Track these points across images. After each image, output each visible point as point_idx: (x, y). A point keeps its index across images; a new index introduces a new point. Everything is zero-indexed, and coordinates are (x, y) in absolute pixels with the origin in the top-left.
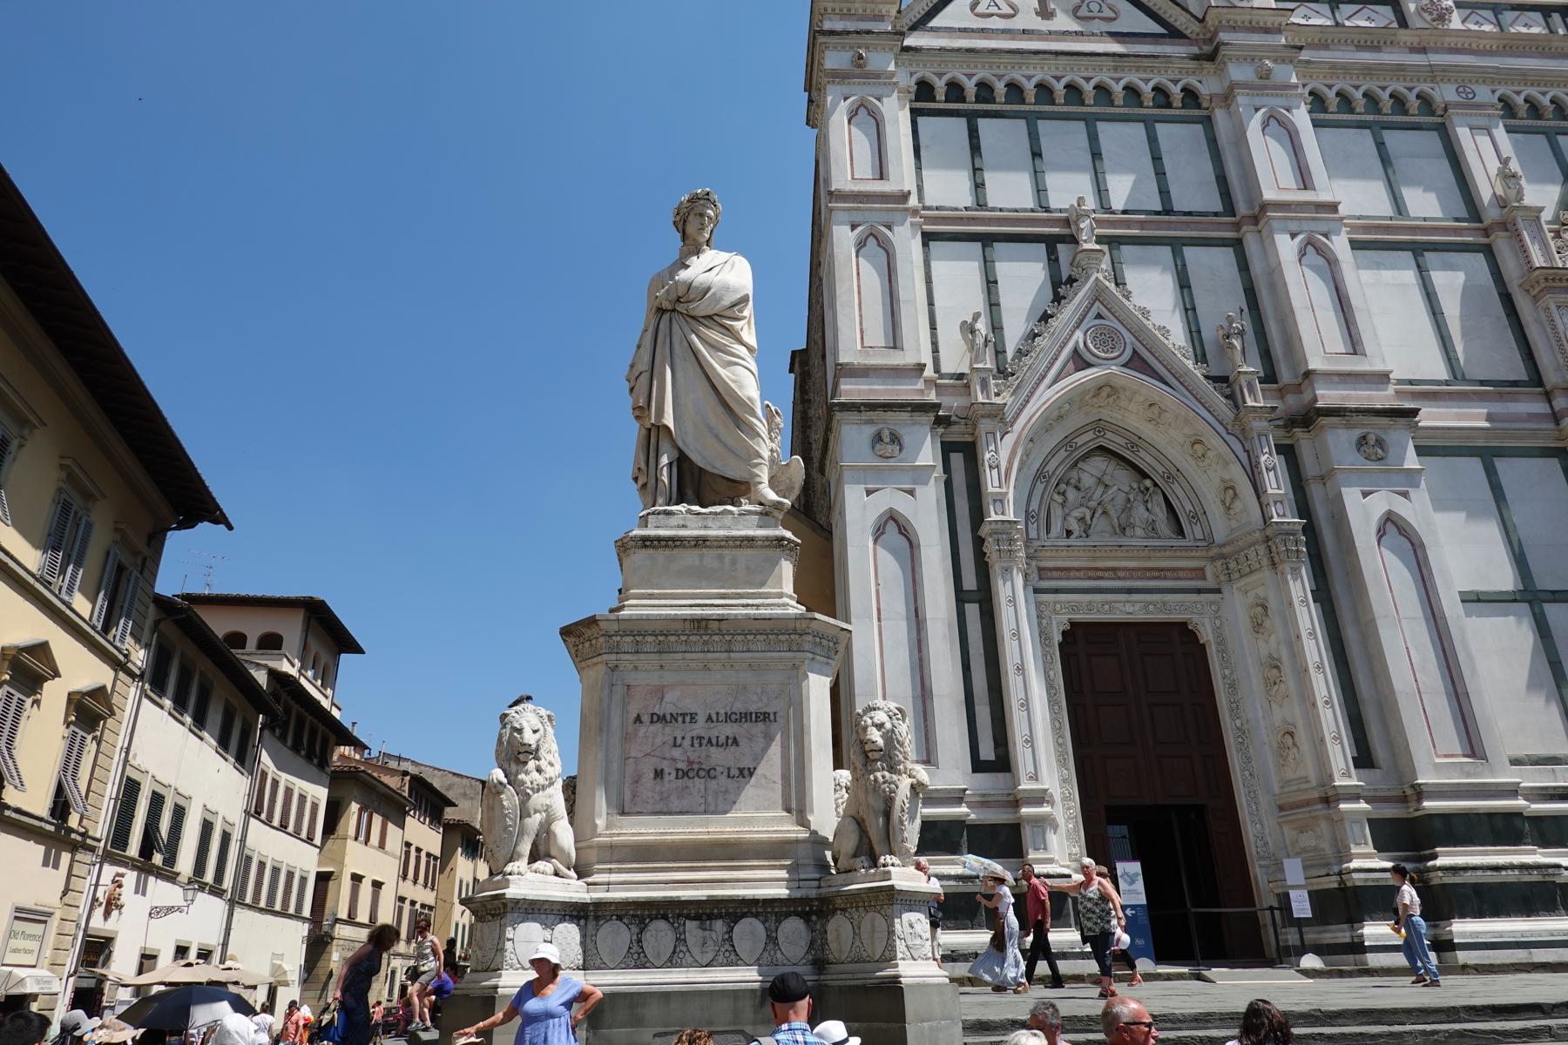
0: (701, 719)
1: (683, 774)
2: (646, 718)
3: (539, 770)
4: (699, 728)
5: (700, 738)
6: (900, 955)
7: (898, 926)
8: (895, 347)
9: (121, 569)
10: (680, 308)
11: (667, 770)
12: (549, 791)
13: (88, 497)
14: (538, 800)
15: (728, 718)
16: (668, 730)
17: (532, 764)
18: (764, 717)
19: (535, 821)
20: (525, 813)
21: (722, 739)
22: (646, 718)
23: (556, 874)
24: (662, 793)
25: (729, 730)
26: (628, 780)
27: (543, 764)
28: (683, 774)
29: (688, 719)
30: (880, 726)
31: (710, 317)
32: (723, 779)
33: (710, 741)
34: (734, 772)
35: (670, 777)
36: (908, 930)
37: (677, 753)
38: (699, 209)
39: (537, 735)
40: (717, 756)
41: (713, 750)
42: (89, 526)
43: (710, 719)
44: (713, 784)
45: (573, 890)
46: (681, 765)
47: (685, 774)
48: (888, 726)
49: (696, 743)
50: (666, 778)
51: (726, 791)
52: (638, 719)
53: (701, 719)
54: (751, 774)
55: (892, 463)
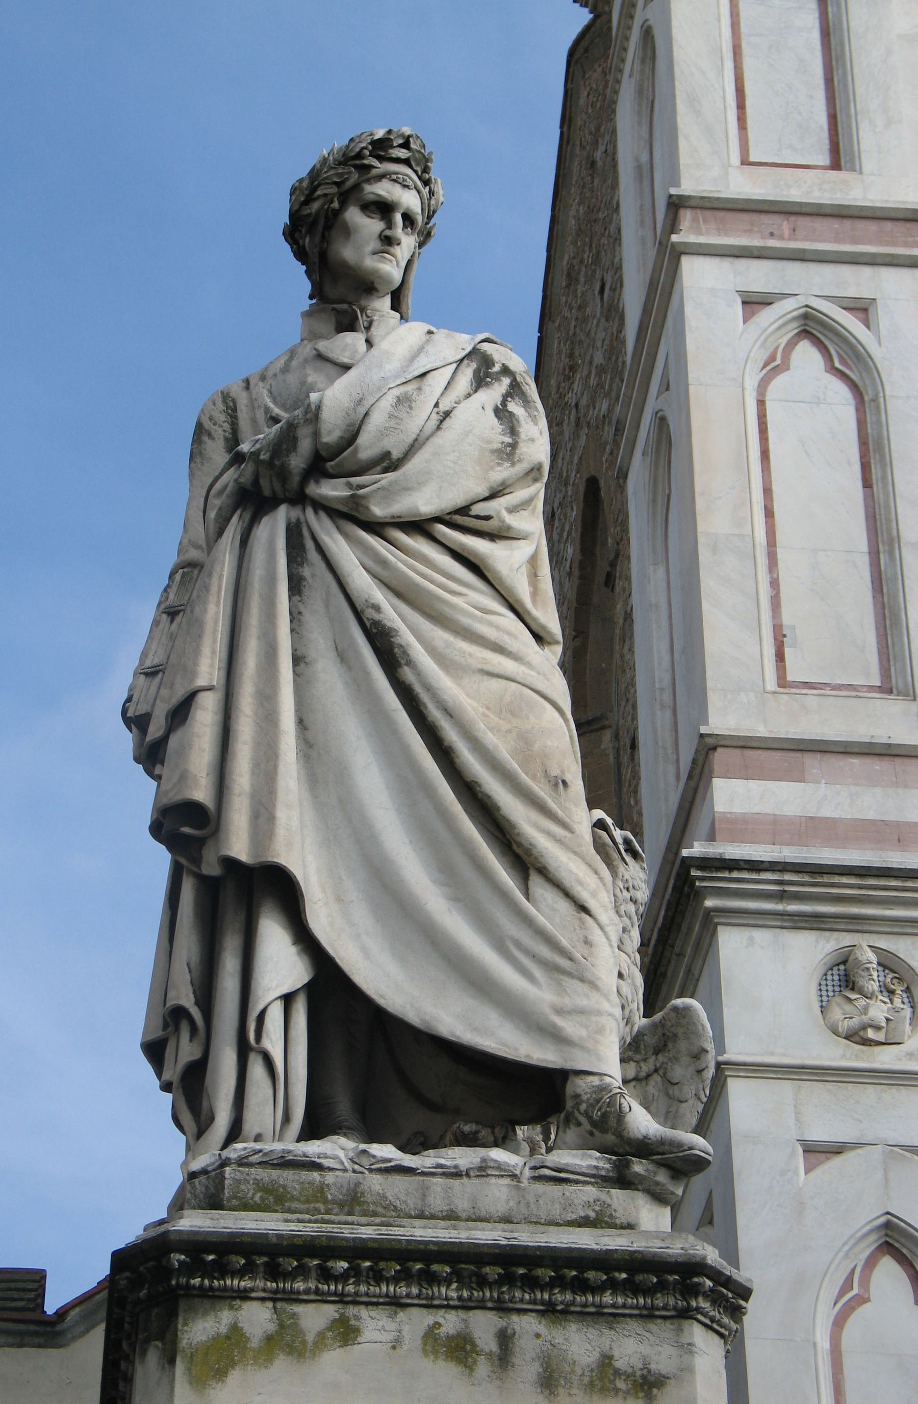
8: (886, 689)
10: (331, 490)
31: (419, 527)
38: (384, 190)
55: (885, 1058)
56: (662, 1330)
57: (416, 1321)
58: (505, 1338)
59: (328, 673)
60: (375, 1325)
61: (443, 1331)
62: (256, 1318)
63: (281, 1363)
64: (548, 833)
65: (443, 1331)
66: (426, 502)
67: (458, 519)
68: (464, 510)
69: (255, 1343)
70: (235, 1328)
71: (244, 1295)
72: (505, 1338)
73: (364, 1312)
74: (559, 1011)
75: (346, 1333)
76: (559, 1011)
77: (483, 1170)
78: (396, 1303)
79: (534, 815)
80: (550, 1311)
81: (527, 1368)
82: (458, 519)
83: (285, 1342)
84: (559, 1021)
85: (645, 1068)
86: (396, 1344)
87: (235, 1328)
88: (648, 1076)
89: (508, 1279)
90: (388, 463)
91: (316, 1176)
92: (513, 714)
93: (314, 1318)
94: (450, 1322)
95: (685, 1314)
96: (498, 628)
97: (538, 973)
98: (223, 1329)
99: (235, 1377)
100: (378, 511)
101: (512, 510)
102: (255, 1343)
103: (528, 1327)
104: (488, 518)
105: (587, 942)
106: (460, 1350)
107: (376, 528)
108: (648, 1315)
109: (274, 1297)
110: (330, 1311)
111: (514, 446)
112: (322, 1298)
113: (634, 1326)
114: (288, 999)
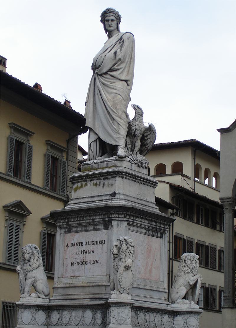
0: (84, 244)
1: (78, 263)
2: (69, 245)
3: (30, 265)
4: (84, 248)
5: (84, 251)
6: (112, 322)
7: (112, 314)
9: (55, 160)
11: (74, 263)
12: (35, 271)
13: (28, 134)
14: (29, 275)
15: (93, 243)
16: (76, 247)
17: (28, 264)
18: (101, 242)
19: (29, 281)
20: (26, 279)
21: (90, 251)
22: (69, 245)
23: (39, 297)
24: (73, 270)
25: (91, 247)
26: (65, 266)
27: (31, 264)
28: (78, 263)
29: (81, 244)
30: (116, 246)
31: (106, 73)
32: (89, 264)
33: (86, 252)
34: (92, 262)
35: (75, 265)
36: (116, 314)
37: (77, 256)
39: (30, 255)
40: (89, 257)
41: (87, 254)
42: (31, 148)
43: (86, 244)
44: (86, 266)
45: (44, 301)
46: (79, 261)
47: (79, 263)
48: (118, 246)
49: (83, 252)
50: (74, 264)
51: (90, 269)
52: (67, 246)
53: (84, 244)
54: (97, 263)
56: (114, 179)
57: (93, 182)
58: (100, 183)
59: (97, 96)
60: (89, 183)
61: (94, 183)
62: (79, 184)
63: (81, 189)
64: (115, 115)
65: (94, 183)
66: (105, 70)
67: (110, 70)
68: (111, 69)
69: (79, 187)
70: (77, 186)
71: (78, 182)
72: (100, 183)
73: (88, 182)
74: (116, 138)
75: (86, 185)
76: (116, 138)
77: (104, 161)
78: (91, 181)
79: (113, 113)
80: (104, 179)
81: (102, 185)
82: (110, 70)
83: (82, 186)
84: (116, 139)
85: (150, 133)
86: (91, 185)
87: (77, 186)
88: (150, 134)
89: (99, 176)
90: (100, 66)
91: (89, 165)
92: (113, 98)
93: (84, 183)
94: (95, 182)
95: (116, 177)
96: (113, 86)
97: (115, 133)
98: (76, 186)
99: (77, 191)
100: (99, 73)
101: (116, 66)
102: (79, 187)
103: (102, 181)
104: (114, 69)
105: (119, 128)
106: (96, 185)
107: (101, 75)
108: (112, 177)
109: (80, 182)
110: (85, 182)
111: (115, 58)
112: (84, 181)
113: (111, 179)
114: (96, 140)
